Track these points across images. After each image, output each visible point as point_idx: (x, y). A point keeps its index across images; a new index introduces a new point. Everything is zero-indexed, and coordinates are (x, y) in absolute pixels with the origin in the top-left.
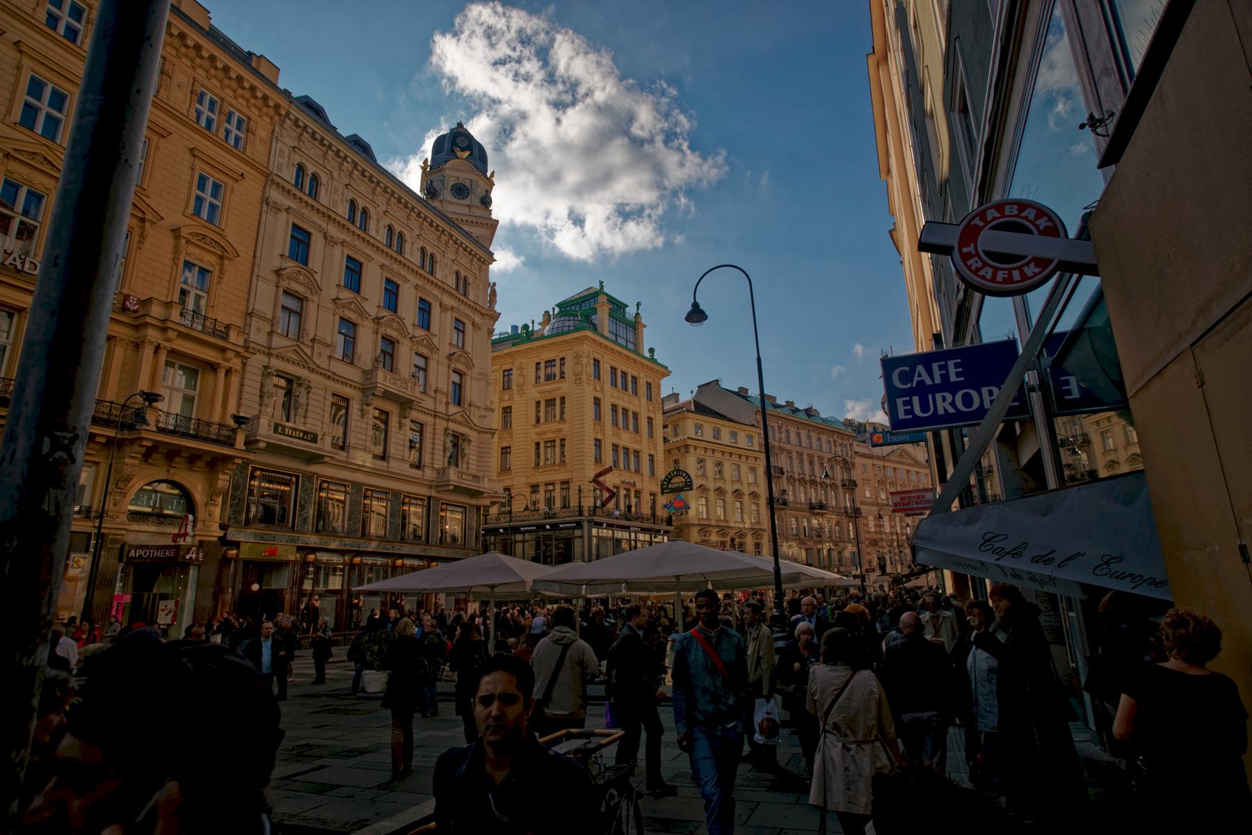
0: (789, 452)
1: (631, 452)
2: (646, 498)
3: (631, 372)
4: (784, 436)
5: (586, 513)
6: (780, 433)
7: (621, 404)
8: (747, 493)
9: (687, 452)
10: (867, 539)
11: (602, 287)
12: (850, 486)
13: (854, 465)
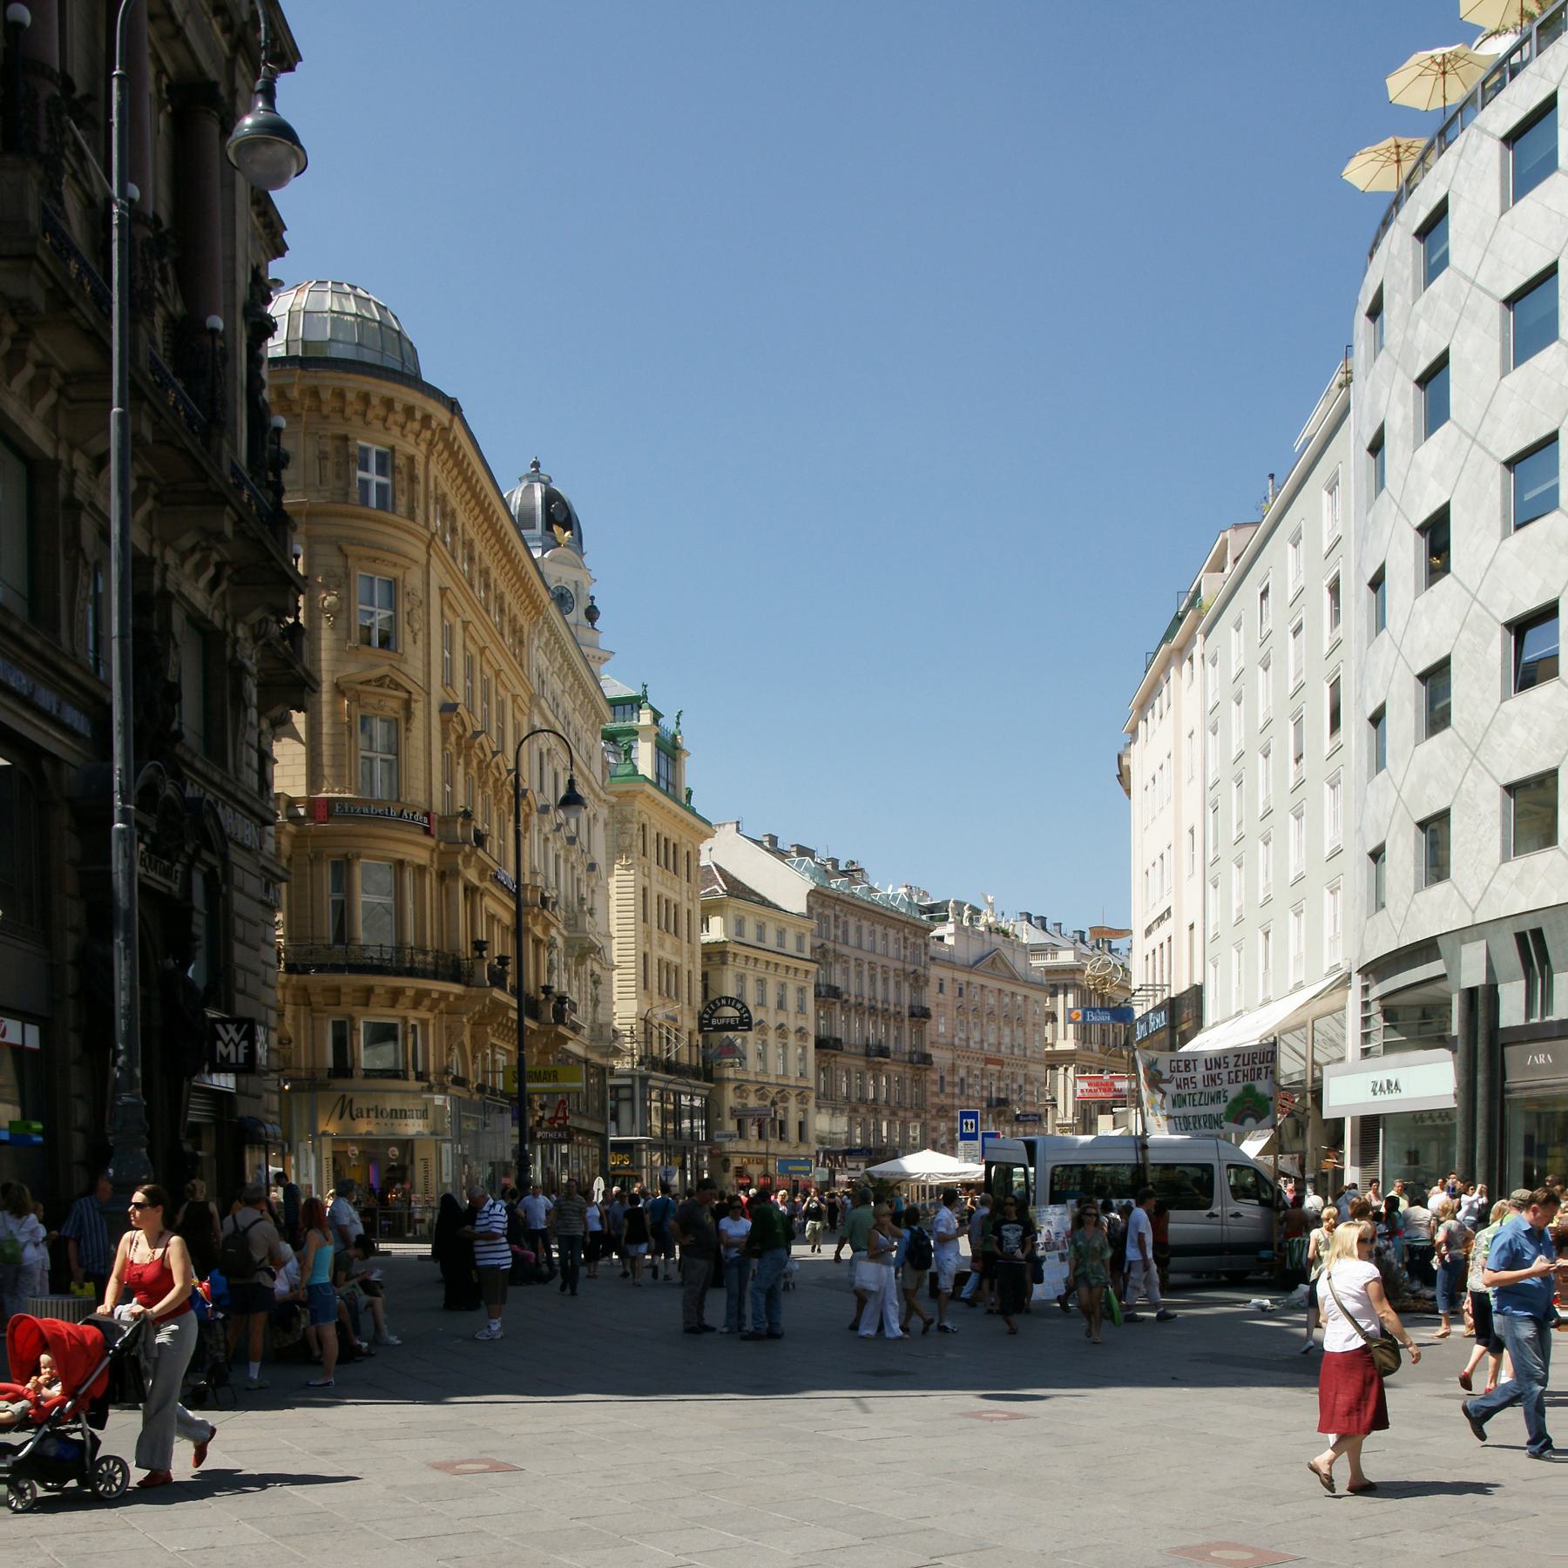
2: (685, 1037)
3: (674, 839)
4: (840, 933)
6: (836, 927)
7: (667, 893)
9: (724, 963)
10: (934, 1105)
11: (645, 697)
13: (927, 982)
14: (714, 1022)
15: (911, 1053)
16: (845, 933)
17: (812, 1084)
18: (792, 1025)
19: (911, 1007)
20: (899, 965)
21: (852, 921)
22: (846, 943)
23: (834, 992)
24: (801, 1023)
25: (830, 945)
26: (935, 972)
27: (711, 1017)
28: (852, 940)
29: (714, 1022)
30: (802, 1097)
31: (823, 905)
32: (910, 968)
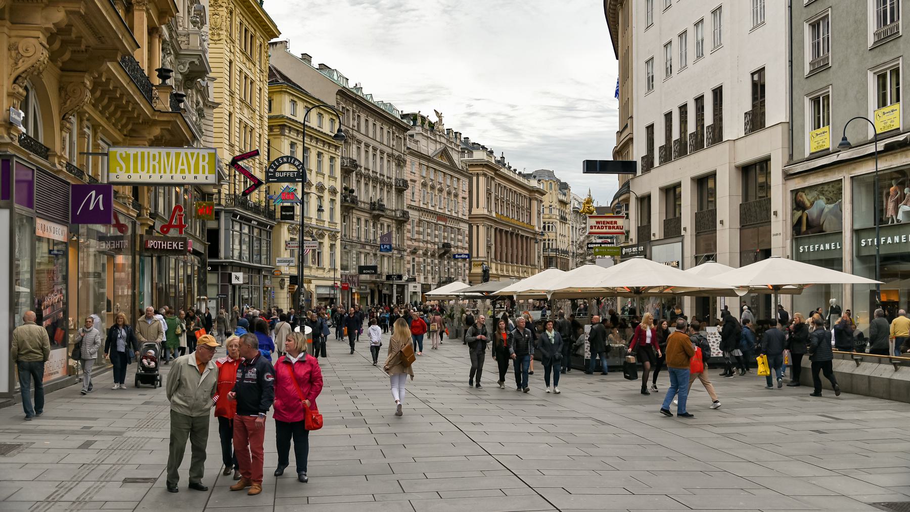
0: (359, 142)
1: (248, 129)
4: (356, 124)
5: (223, 202)
6: (354, 119)
8: (327, 187)
10: (409, 246)
12: (401, 188)
13: (405, 161)
14: (277, 175)
15: (395, 211)
16: (359, 124)
17: (339, 228)
18: (327, 184)
19: (396, 179)
20: (389, 151)
21: (363, 117)
22: (359, 131)
23: (354, 164)
24: (332, 183)
25: (351, 131)
26: (409, 158)
27: (275, 171)
28: (363, 130)
29: (277, 175)
30: (333, 237)
31: (345, 103)
32: (396, 154)
